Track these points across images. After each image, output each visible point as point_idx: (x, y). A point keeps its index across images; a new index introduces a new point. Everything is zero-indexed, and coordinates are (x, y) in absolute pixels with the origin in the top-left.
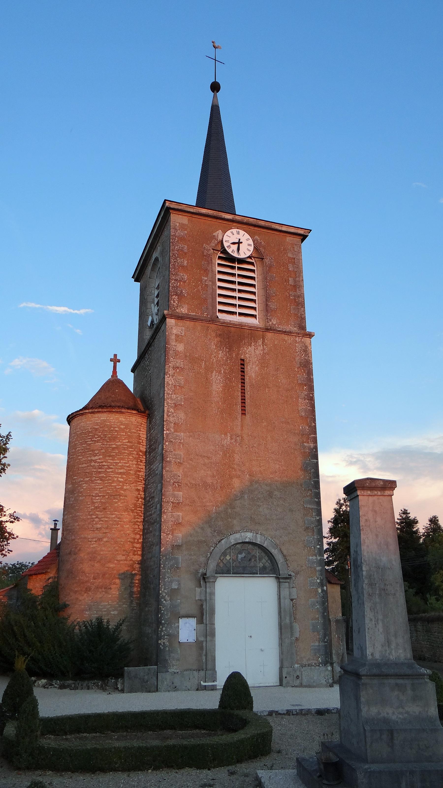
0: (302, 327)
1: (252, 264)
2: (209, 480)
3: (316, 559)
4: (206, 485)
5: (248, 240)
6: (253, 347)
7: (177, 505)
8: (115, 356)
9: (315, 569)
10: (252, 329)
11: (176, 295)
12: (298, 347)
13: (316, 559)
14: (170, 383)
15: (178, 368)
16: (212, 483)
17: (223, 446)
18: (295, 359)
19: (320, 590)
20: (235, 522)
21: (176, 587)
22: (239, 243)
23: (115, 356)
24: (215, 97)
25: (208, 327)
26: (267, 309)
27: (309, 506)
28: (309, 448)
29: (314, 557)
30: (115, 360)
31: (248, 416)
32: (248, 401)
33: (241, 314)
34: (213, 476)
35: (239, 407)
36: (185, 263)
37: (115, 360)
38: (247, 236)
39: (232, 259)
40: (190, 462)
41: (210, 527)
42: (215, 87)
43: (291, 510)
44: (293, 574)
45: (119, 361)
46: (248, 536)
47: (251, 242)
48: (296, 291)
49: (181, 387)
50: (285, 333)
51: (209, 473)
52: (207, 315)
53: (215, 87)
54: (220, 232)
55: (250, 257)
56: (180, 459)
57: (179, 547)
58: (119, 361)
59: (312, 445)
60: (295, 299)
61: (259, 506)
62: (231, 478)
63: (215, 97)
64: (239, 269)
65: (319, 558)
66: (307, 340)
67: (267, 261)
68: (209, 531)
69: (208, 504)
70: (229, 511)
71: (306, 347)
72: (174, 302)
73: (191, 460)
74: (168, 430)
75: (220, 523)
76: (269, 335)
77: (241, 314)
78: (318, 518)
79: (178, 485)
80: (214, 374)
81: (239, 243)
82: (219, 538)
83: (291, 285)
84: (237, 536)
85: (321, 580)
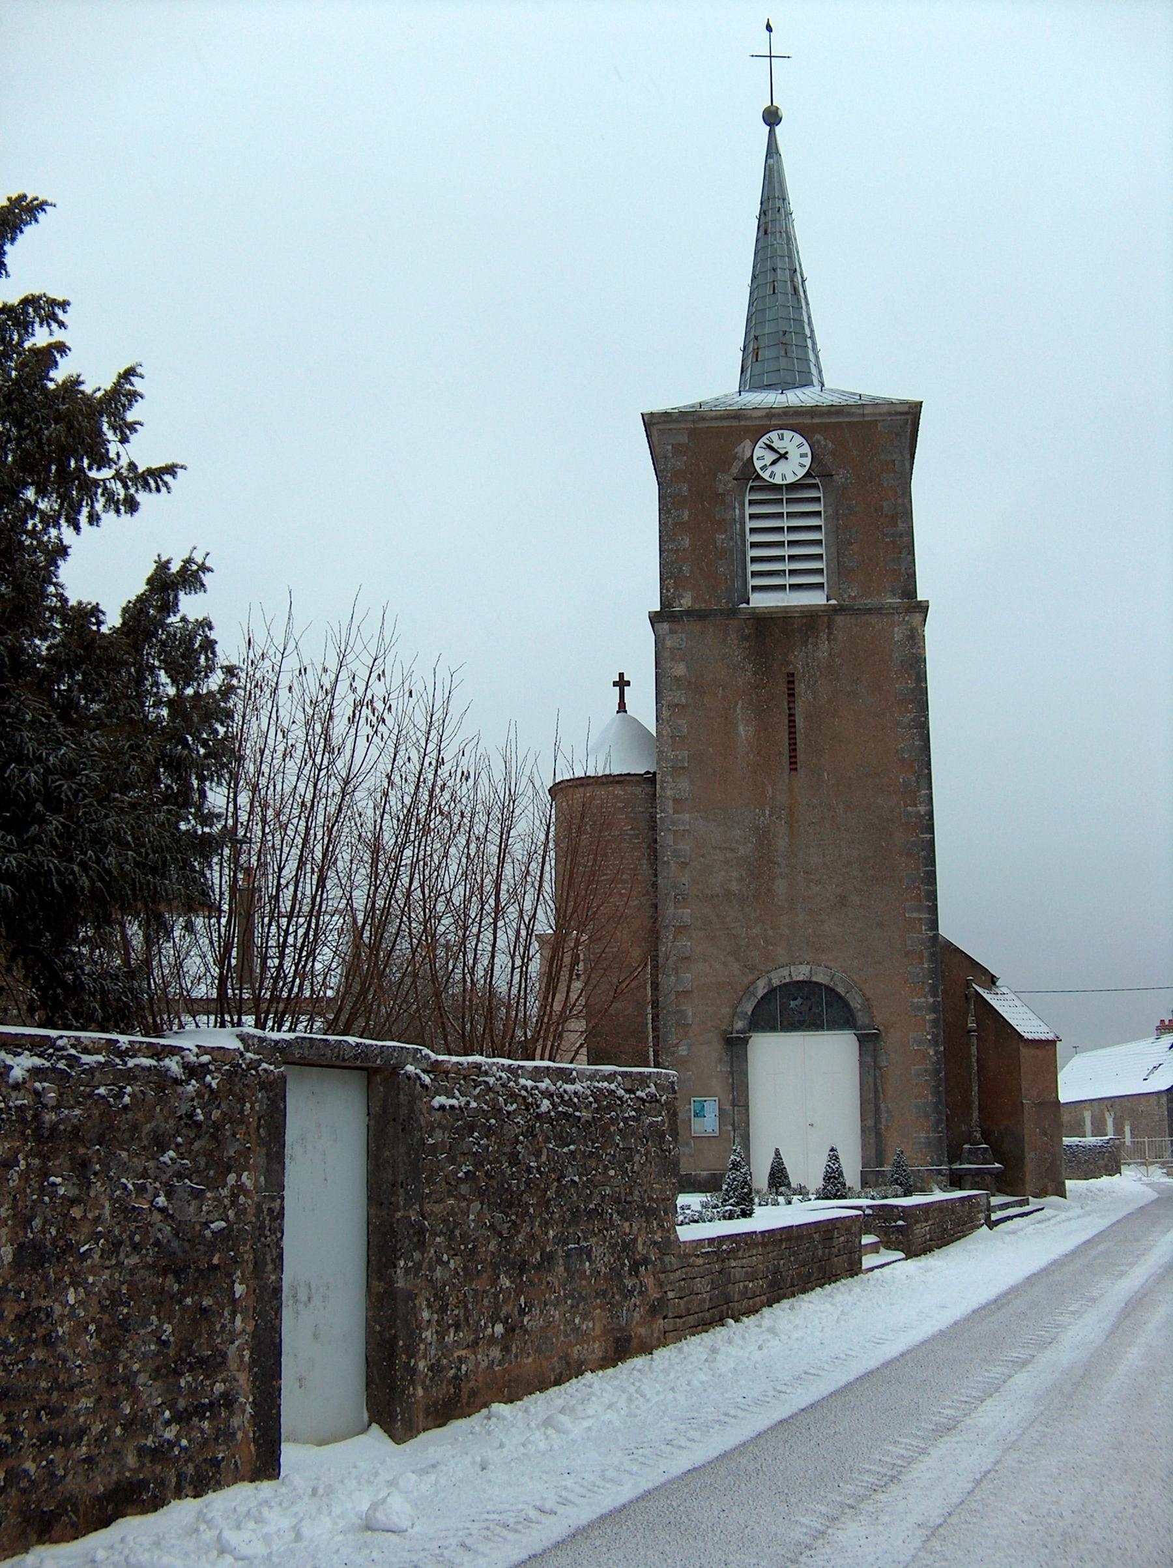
0: (909, 591)
1: (815, 486)
2: (734, 887)
3: (926, 1002)
4: (728, 894)
5: (800, 446)
6: (810, 646)
7: (682, 929)
8: (621, 675)
9: (924, 1019)
10: (810, 616)
11: (670, 578)
12: (898, 634)
13: (926, 1002)
14: (664, 733)
15: (677, 705)
16: (740, 890)
17: (757, 828)
18: (891, 657)
19: (931, 1052)
20: (779, 950)
21: (685, 1053)
22: (784, 456)
23: (621, 675)
24: (772, 134)
25: (727, 625)
26: (841, 573)
27: (915, 915)
28: (918, 814)
29: (923, 1000)
30: (622, 683)
31: (801, 771)
32: (801, 745)
33: (793, 587)
34: (741, 879)
35: (785, 760)
36: (686, 518)
37: (622, 683)
38: (799, 439)
39: (776, 488)
40: (702, 860)
41: (737, 960)
42: (772, 117)
43: (880, 925)
44: (881, 1028)
45: (628, 683)
46: (801, 973)
47: (806, 449)
48: (896, 526)
49: (682, 738)
50: (869, 611)
51: (735, 874)
52: (727, 603)
53: (772, 117)
54: (748, 443)
55: (808, 475)
56: (684, 857)
57: (686, 993)
58: (628, 683)
59: (922, 809)
60: (893, 542)
61: (823, 922)
62: (773, 879)
63: (772, 134)
64: (789, 501)
65: (931, 1000)
66: (918, 617)
67: (839, 479)
68: (735, 967)
69: (734, 925)
70: (770, 932)
71: (912, 629)
72: (668, 591)
73: (703, 856)
74: (662, 812)
75: (755, 953)
76: (839, 620)
77: (793, 587)
78: (931, 934)
79: (682, 899)
80: (740, 706)
81: (784, 456)
82: (751, 977)
83: (886, 516)
84: (784, 972)
85: (935, 1036)
